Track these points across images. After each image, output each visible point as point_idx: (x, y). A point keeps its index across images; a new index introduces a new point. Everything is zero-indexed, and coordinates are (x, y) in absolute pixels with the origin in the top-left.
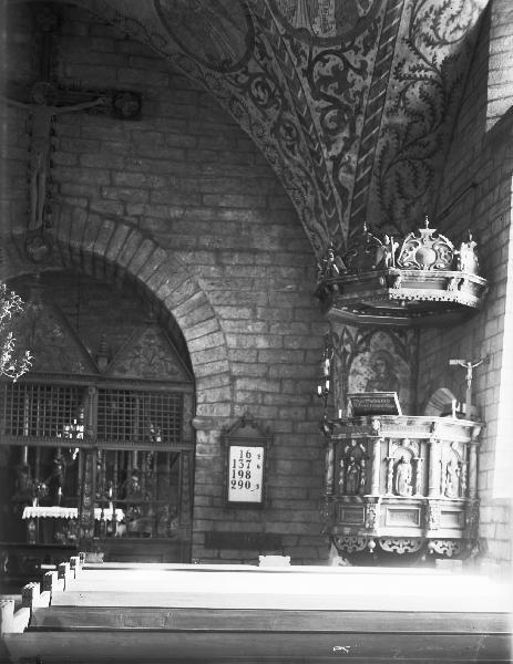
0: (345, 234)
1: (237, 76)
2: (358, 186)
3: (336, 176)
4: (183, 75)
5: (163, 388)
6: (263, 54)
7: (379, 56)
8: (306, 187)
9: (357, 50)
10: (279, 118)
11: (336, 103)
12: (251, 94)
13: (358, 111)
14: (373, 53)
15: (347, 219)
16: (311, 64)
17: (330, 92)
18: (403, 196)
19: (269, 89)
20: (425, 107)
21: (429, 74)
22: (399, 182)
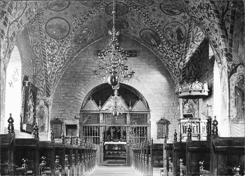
0: (181, 79)
2: (183, 69)
3: (179, 67)
7: (187, 44)
8: (172, 69)
9: (182, 43)
10: (166, 56)
11: (178, 53)
13: (183, 54)
14: (185, 44)
15: (181, 76)
16: (172, 46)
17: (177, 51)
18: (193, 70)
20: (197, 53)
21: (197, 47)
22: (192, 67)
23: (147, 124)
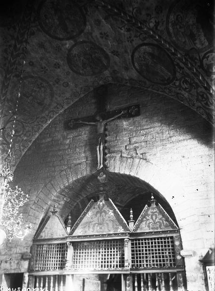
1: (175, 83)
4: (156, 93)
5: (163, 236)
6: (181, 68)
10: (197, 93)
12: (183, 88)
16: (201, 61)
19: (188, 82)
23: (174, 265)
